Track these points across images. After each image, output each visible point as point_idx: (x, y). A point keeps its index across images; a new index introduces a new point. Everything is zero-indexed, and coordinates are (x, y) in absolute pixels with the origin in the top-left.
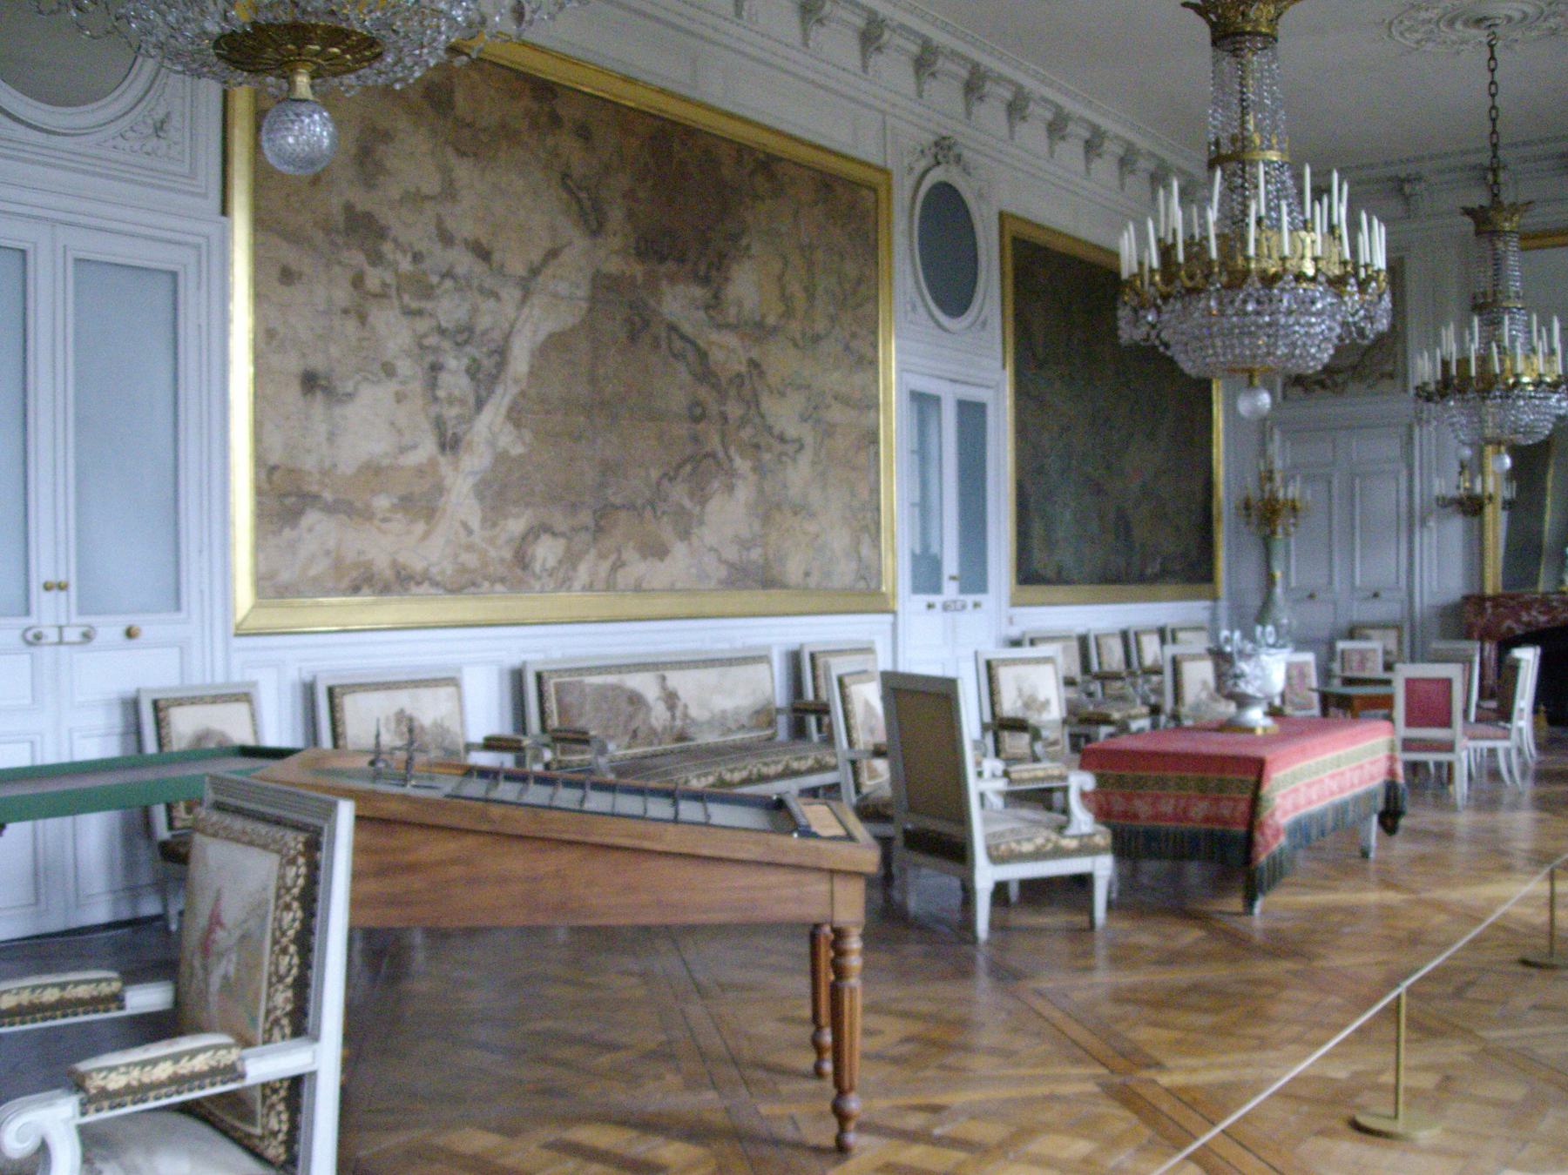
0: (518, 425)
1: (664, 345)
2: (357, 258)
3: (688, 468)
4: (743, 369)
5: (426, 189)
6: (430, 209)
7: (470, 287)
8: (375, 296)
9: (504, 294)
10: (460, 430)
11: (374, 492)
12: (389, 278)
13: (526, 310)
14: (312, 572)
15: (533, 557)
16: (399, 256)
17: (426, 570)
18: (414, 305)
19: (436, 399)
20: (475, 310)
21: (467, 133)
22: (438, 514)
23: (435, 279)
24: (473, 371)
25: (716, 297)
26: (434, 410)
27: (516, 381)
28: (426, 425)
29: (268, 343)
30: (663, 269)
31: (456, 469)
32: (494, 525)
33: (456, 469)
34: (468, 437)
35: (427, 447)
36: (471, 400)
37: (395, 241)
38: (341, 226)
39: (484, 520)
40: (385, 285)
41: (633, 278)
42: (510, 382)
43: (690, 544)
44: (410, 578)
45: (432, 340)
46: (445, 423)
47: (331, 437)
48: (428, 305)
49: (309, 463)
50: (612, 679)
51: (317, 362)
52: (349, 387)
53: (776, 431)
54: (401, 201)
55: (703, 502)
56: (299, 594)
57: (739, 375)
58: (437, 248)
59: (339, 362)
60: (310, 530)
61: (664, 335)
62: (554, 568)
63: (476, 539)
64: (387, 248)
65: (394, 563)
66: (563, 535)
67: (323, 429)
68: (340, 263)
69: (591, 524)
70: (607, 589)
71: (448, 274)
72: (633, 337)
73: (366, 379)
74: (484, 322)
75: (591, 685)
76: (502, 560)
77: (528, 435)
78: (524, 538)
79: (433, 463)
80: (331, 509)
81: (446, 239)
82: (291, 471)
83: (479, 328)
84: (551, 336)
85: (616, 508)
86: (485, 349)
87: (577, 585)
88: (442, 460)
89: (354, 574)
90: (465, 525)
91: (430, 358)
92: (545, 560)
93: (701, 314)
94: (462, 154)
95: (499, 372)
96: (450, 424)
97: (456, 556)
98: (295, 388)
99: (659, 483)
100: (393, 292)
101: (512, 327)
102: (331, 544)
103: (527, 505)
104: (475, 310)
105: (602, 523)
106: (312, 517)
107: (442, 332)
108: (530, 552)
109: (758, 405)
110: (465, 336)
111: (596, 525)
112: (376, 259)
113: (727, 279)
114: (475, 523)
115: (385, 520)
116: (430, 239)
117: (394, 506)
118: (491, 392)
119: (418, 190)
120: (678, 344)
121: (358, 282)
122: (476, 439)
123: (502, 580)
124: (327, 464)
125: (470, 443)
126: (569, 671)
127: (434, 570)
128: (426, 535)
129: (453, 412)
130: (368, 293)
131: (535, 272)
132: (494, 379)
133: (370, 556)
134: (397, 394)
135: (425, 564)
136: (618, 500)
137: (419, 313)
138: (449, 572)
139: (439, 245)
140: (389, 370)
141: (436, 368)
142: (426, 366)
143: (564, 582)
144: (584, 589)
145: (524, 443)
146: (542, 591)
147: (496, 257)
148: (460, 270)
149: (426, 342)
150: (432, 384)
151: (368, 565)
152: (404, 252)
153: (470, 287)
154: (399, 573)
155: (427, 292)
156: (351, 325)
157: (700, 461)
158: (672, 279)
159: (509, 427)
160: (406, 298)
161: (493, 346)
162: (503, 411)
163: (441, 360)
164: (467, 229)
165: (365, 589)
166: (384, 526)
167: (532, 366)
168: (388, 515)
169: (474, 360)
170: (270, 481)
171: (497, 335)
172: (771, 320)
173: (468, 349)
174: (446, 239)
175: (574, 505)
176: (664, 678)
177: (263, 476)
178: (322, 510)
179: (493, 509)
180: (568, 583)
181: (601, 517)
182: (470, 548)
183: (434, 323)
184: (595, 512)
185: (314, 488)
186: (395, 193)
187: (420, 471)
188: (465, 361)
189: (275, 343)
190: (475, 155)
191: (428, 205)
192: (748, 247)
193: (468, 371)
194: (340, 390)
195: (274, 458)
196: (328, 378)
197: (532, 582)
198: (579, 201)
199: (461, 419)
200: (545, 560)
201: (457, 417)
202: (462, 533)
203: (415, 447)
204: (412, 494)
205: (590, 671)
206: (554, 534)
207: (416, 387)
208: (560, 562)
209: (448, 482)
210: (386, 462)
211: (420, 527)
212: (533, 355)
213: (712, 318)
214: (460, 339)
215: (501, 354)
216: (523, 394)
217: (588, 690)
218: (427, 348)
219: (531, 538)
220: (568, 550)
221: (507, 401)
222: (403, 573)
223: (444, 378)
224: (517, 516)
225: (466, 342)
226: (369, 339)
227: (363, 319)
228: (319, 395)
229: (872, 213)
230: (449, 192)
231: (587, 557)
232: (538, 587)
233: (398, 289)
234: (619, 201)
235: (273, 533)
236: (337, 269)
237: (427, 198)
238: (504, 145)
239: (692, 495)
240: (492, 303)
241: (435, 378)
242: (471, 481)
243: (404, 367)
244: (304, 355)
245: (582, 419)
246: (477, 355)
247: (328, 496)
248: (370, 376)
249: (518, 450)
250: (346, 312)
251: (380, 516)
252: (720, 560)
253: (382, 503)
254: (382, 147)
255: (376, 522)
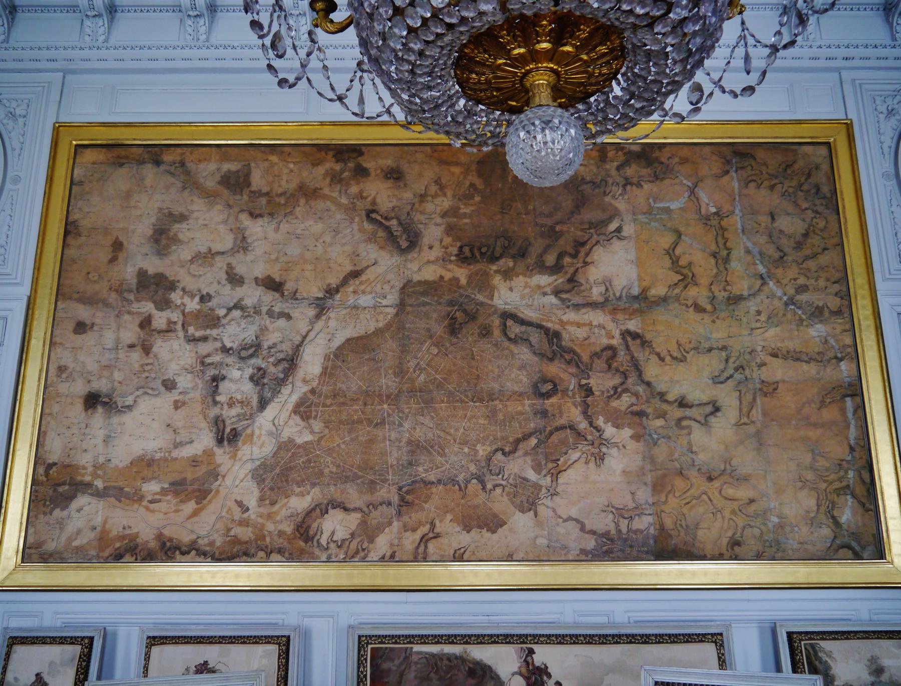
0: (306, 417)
1: (497, 333)
2: (148, 307)
3: (533, 441)
4: (616, 341)
5: (218, 247)
6: (220, 263)
7: (257, 312)
8: (159, 332)
9: (295, 314)
10: (240, 426)
11: (145, 480)
12: (176, 316)
13: (320, 324)
14: (75, 544)
15: (319, 531)
16: (187, 300)
17: (194, 542)
18: (199, 334)
19: (215, 403)
20: (263, 330)
21: (264, 201)
22: (209, 497)
23: (222, 312)
24: (258, 378)
25: (571, 280)
26: (214, 411)
27: (305, 381)
28: (204, 425)
29: (58, 376)
30: (494, 268)
31: (234, 457)
32: (273, 503)
33: (234, 457)
34: (249, 431)
35: (205, 440)
36: (255, 401)
37: (183, 289)
38: (134, 286)
39: (261, 499)
40: (170, 322)
41: (457, 280)
42: (299, 383)
43: (536, 515)
44: (177, 548)
45: (217, 358)
46: (223, 421)
47: (107, 440)
48: (214, 332)
49: (85, 460)
50: (448, 649)
51: (101, 385)
52: (129, 401)
53: (670, 397)
54: (192, 261)
55: (556, 475)
56: (63, 560)
57: (610, 348)
58: (227, 289)
59: (120, 383)
60: (79, 510)
61: (497, 322)
62: (344, 540)
63: (252, 515)
64: (176, 297)
65: (160, 536)
66: (355, 510)
67: (101, 434)
68: (129, 313)
69: (396, 499)
70: (415, 559)
71: (237, 306)
72: (453, 329)
73: (146, 393)
74: (272, 338)
75: (419, 653)
76: (281, 533)
77: (317, 425)
78: (309, 513)
79: (209, 454)
80: (100, 494)
81: (235, 280)
82: (68, 466)
83: (265, 345)
84: (348, 341)
85: (427, 484)
86: (271, 360)
87: (374, 556)
88: (218, 451)
89: (118, 545)
90: (240, 504)
91: (212, 372)
92: (333, 533)
93: (553, 299)
94: (254, 215)
95: (287, 377)
96: (228, 422)
97: (229, 530)
98: (79, 406)
99: (489, 460)
100: (179, 327)
101: (305, 337)
102: (98, 521)
103: (314, 485)
104: (263, 330)
105: (409, 498)
106: (82, 500)
107: (226, 350)
108: (315, 525)
109: (640, 373)
110: (251, 351)
111: (402, 499)
112: (164, 304)
113: (586, 264)
114: (252, 502)
115: (151, 502)
116: (219, 283)
117: (162, 488)
118: (276, 392)
119: (210, 250)
120: (515, 329)
121: (146, 323)
122: (257, 432)
123: (280, 551)
124: (101, 460)
125: (252, 434)
126: (395, 638)
127: (200, 541)
128: (195, 513)
129: (235, 411)
130: (154, 330)
131: (331, 292)
132: (281, 382)
133: (135, 531)
134: (176, 402)
135: (194, 537)
136: (432, 477)
137: (205, 339)
138: (218, 544)
139: (228, 287)
140: (169, 385)
141: (217, 380)
142: (207, 377)
143: (357, 552)
144: (383, 559)
145: (312, 432)
146: (329, 560)
147: (289, 286)
148: (248, 302)
149: (208, 360)
150: (215, 391)
151: (133, 538)
152: (192, 296)
153: (257, 312)
154: (164, 544)
155: (214, 322)
156: (136, 356)
157: (551, 433)
158: (507, 275)
159: (297, 418)
160: (191, 330)
161: (281, 356)
162: (290, 406)
163: (224, 372)
164: (260, 271)
165: (127, 558)
166: (152, 506)
167: (325, 369)
168: (157, 497)
169: (259, 369)
170: (47, 473)
171: (287, 347)
172: (659, 291)
173: (257, 361)
174: (235, 280)
175: (372, 483)
176: (531, 652)
177: (41, 470)
178: (92, 495)
179: (272, 489)
180: (362, 554)
181: (408, 493)
182: (244, 523)
183: (218, 345)
184: (400, 489)
185: (88, 478)
186: (186, 254)
187: (194, 462)
188: (250, 371)
189: (64, 376)
190: (271, 214)
191: (218, 258)
192: (619, 230)
193: (251, 378)
194: (120, 404)
195: (53, 458)
196: (109, 396)
197: (317, 552)
198: (387, 229)
199: (241, 417)
200: (333, 533)
201: (238, 415)
202: (237, 510)
203: (192, 442)
204: (185, 479)
205: (424, 639)
206: (346, 509)
207: (197, 395)
208: (353, 535)
209: (223, 470)
210: (158, 456)
211: (191, 506)
212: (327, 358)
213: (563, 300)
214: (244, 354)
215: (291, 363)
216: (313, 391)
217: (415, 658)
218: (209, 364)
219: (314, 514)
220: (363, 523)
221: (295, 398)
222: (168, 544)
223: (224, 386)
224: (302, 495)
225: (251, 356)
226: (151, 364)
227: (147, 350)
228: (100, 409)
229: (825, 167)
230: (242, 245)
231: (387, 530)
232: (324, 558)
233: (183, 325)
234: (439, 220)
235: (45, 514)
236: (126, 317)
237: (219, 253)
238: (302, 201)
239: (537, 468)
240: (282, 322)
241: (217, 386)
242: (249, 466)
243: (184, 382)
244: (89, 382)
245: (385, 406)
246: (263, 366)
247: (99, 484)
248: (150, 392)
249: (308, 437)
250: (132, 346)
251: (150, 498)
252: (583, 528)
253: (152, 488)
254: (177, 226)
255: (145, 503)
